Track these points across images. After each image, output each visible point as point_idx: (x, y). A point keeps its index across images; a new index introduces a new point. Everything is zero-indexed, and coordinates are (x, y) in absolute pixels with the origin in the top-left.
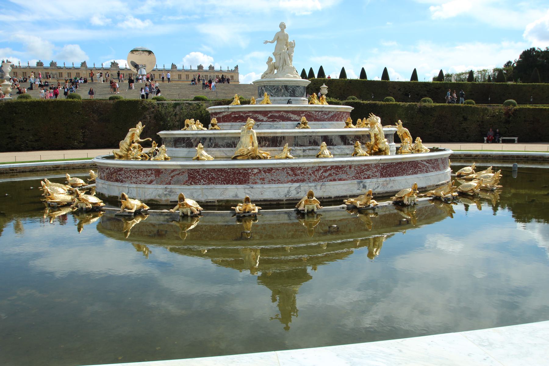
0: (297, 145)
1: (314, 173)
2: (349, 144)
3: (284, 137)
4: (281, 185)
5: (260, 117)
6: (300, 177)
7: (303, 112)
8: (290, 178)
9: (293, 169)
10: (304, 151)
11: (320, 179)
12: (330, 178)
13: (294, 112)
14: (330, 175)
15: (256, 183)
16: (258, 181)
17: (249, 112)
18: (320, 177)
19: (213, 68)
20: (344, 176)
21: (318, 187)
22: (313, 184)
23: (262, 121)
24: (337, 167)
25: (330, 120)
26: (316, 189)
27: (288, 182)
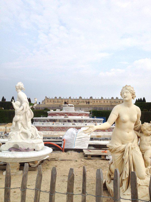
0: (60, 122)
1: (56, 129)
2: (76, 122)
3: (57, 120)
4: (47, 131)
5: (57, 114)
6: (52, 130)
7: (68, 113)
8: (50, 130)
9: (50, 127)
10: (62, 123)
11: (58, 130)
12: (60, 130)
13: (66, 113)
14: (61, 129)
15: (41, 131)
16: (42, 130)
17: (55, 113)
18: (58, 130)
19: (118, 98)
20: (65, 130)
21: (57, 133)
22: (55, 132)
23: (57, 115)
24: (63, 127)
25: (77, 116)
26: (56, 133)
27: (49, 131)
